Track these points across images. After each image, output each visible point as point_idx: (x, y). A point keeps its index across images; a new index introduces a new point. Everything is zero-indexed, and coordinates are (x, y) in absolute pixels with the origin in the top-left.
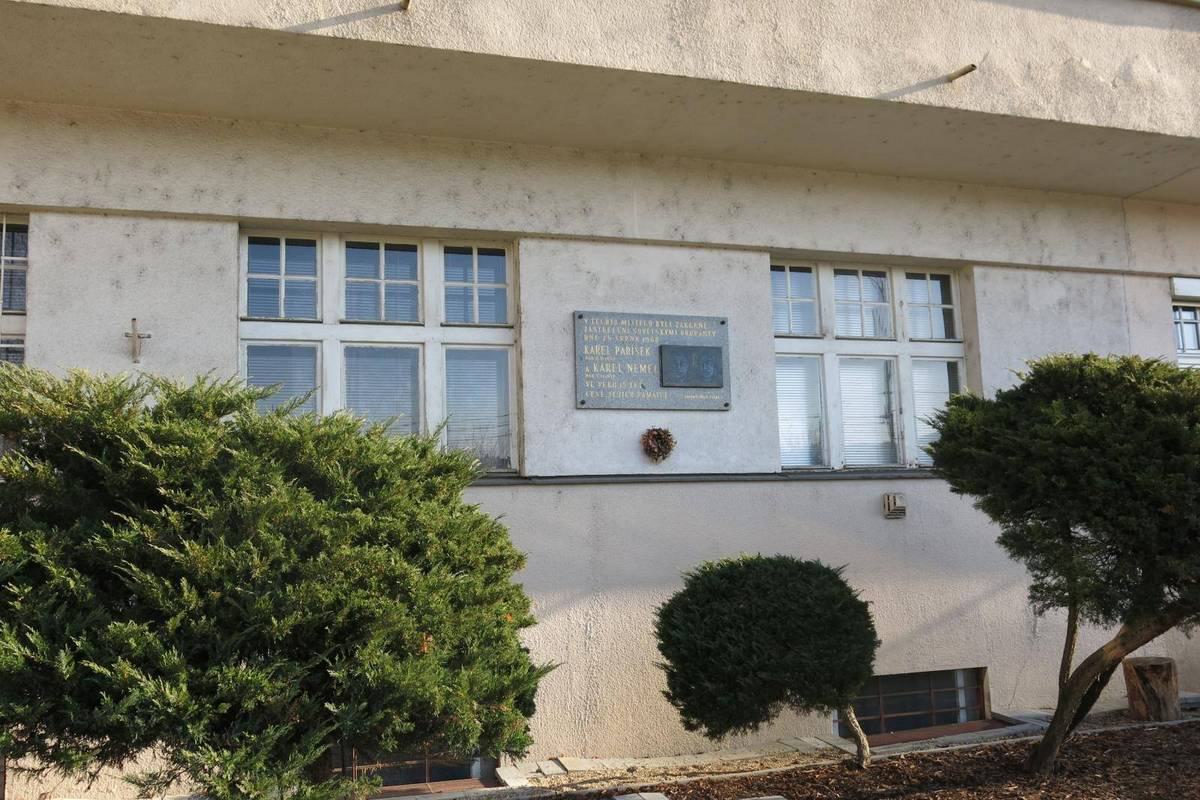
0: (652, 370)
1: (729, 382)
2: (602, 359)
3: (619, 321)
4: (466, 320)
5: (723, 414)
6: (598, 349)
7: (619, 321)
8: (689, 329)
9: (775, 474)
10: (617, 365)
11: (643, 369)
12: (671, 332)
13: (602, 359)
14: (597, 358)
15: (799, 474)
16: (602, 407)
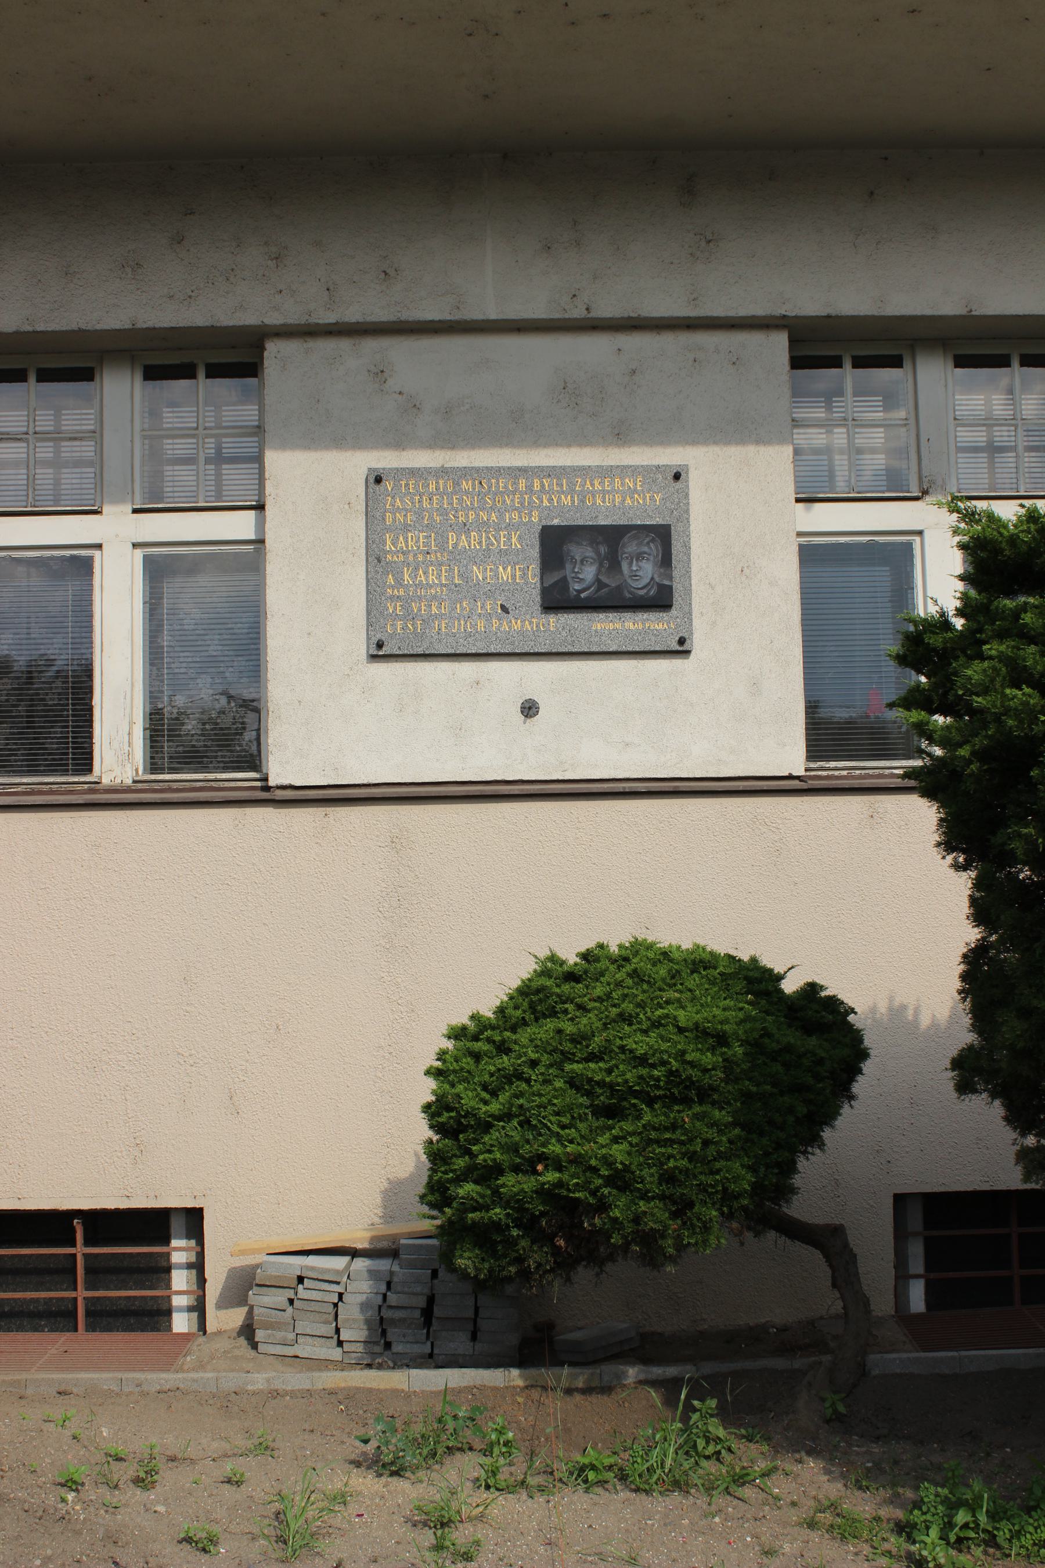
0: (524, 576)
1: (688, 591)
2: (420, 558)
3: (457, 484)
4: (219, 497)
5: (677, 663)
6: (414, 541)
7: (457, 484)
8: (604, 492)
9: (790, 777)
10: (450, 570)
11: (505, 574)
12: (566, 500)
13: (420, 558)
14: (411, 558)
15: (860, 777)
16: (420, 651)
